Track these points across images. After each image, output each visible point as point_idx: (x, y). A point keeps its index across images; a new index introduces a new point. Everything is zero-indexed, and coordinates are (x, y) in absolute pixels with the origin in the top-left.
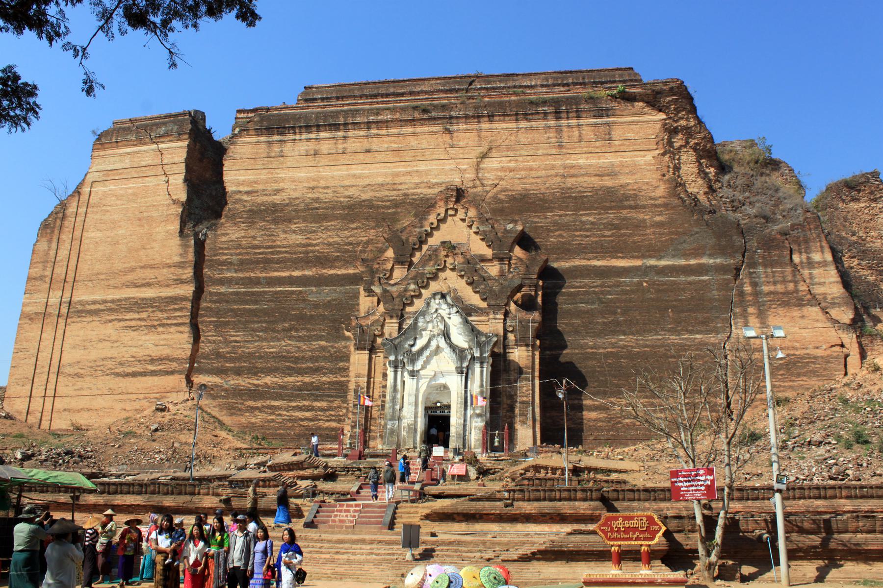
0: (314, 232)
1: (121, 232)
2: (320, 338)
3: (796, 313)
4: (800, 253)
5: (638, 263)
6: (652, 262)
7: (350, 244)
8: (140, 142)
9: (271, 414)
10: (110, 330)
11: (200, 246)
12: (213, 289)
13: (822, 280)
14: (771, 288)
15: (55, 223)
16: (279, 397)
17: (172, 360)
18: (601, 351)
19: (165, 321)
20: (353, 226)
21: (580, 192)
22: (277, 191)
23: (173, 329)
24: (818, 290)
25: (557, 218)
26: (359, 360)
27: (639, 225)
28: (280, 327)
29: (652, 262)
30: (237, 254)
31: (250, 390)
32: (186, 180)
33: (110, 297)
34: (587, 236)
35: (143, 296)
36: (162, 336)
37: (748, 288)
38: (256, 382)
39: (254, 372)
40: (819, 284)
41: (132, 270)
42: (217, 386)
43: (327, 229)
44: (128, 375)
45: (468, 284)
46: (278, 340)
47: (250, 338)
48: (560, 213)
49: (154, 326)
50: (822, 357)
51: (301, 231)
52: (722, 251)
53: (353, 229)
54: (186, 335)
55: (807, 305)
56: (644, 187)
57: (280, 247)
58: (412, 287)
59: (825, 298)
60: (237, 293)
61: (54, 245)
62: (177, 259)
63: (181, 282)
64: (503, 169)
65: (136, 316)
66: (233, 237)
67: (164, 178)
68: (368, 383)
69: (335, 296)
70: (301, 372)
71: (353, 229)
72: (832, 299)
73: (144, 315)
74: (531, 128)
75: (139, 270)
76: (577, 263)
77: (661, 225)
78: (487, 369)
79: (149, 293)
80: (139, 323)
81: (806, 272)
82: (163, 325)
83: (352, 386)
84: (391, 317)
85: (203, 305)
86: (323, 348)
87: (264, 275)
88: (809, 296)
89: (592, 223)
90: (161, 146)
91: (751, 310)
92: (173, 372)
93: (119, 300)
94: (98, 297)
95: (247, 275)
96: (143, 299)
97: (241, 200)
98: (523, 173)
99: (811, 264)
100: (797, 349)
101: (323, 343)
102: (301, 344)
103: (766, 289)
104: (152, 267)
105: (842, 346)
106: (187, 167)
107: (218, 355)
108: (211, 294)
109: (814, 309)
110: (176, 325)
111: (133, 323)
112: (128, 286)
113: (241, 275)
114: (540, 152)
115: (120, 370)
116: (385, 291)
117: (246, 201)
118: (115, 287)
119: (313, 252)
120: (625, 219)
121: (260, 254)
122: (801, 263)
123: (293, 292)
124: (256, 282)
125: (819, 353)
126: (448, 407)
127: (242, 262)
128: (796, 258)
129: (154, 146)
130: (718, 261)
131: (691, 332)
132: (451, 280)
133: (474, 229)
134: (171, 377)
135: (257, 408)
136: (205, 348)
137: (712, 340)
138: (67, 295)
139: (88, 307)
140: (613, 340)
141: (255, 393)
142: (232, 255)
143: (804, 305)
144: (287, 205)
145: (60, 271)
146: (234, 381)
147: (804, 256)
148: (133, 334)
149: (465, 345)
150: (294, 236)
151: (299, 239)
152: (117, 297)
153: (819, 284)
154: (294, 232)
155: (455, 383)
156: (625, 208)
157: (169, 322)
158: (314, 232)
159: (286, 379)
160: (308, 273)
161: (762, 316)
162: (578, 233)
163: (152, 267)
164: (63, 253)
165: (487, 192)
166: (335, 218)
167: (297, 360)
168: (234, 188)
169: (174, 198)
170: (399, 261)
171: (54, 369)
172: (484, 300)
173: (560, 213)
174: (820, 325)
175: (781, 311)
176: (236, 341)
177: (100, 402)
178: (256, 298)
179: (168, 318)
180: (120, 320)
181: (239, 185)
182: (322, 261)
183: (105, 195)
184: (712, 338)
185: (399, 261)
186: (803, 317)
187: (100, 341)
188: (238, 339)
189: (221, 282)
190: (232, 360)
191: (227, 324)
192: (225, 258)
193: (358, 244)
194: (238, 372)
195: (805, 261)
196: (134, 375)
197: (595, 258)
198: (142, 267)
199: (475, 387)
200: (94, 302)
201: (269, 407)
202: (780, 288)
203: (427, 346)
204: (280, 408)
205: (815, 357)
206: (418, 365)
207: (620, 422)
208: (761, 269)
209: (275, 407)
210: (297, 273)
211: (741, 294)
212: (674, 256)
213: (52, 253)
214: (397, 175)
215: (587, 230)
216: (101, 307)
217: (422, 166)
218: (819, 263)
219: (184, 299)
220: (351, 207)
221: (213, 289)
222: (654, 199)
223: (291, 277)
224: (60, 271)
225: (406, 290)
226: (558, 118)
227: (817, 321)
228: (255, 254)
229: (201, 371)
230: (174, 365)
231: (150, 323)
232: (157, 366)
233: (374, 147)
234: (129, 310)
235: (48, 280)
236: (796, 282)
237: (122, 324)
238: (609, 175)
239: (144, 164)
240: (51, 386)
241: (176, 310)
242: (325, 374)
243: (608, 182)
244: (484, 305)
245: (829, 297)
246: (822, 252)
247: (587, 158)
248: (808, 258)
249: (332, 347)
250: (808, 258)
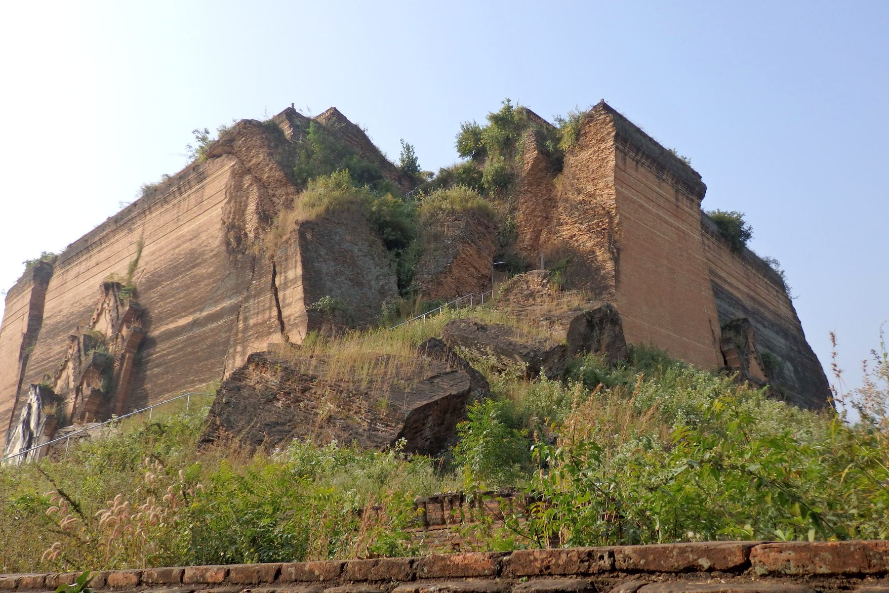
5: (190, 319)
6: (198, 315)
29: (198, 315)
34: (172, 302)
52: (237, 290)
55: (273, 332)
59: (289, 320)
72: (295, 319)
76: (163, 329)
77: (210, 275)
103: (251, 322)
120: (195, 276)
147: (283, 278)
212: (210, 305)
226: (181, 194)
238: (195, 237)
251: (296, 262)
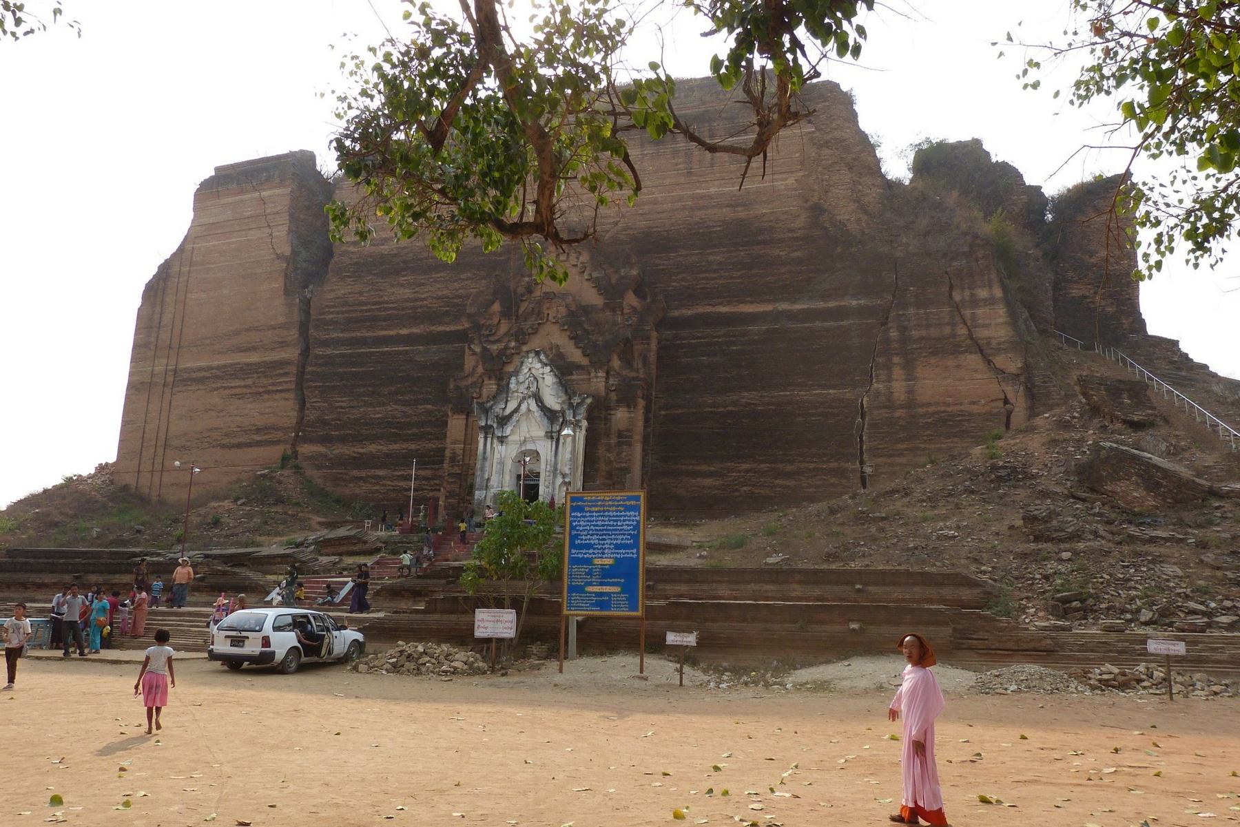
0: (423, 284)
1: (225, 292)
2: (427, 401)
3: (951, 362)
4: (963, 289)
5: (768, 308)
6: (784, 306)
7: (460, 297)
8: (242, 192)
9: (374, 484)
11: (307, 303)
12: (319, 351)
13: (987, 322)
14: (923, 333)
16: (383, 466)
17: (277, 429)
18: (721, 409)
19: (271, 388)
20: (463, 276)
21: (708, 227)
23: (278, 396)
24: (981, 334)
25: (681, 259)
26: (456, 424)
29: (784, 306)
30: (343, 312)
31: (354, 458)
32: (290, 231)
33: (215, 363)
35: (248, 360)
36: (268, 404)
37: (894, 334)
38: (361, 451)
39: (360, 439)
40: (983, 326)
41: (237, 333)
42: (321, 455)
43: (435, 281)
45: (571, 338)
46: (384, 404)
47: (356, 404)
48: (684, 252)
49: (260, 394)
50: (979, 414)
53: (463, 280)
54: (291, 403)
56: (783, 217)
57: (387, 302)
58: (513, 344)
59: (989, 343)
60: (343, 355)
61: (158, 309)
62: (282, 319)
63: (284, 344)
65: (242, 383)
66: (341, 292)
67: (268, 231)
68: (464, 449)
70: (406, 439)
71: (463, 280)
72: (999, 344)
73: (249, 382)
78: (581, 435)
79: (254, 358)
80: (245, 390)
81: (967, 313)
82: (269, 392)
83: (448, 453)
84: (490, 378)
85: (309, 369)
86: (429, 412)
87: (370, 334)
88: (968, 342)
89: (720, 263)
90: (263, 194)
91: (896, 359)
92: (278, 442)
93: (225, 366)
94: (202, 364)
95: (353, 335)
96: (248, 364)
97: (346, 252)
99: (975, 302)
100: (949, 405)
101: (429, 407)
102: (406, 409)
103: (915, 333)
104: (256, 329)
105: (1006, 401)
106: (292, 216)
107: (325, 423)
108: (317, 357)
109: (973, 356)
110: (281, 391)
111: (238, 391)
112: (233, 351)
113: (347, 335)
114: (667, 181)
115: (226, 441)
116: (484, 349)
117: (353, 253)
118: (220, 353)
119: (421, 307)
121: (366, 311)
122: (963, 300)
123: (399, 353)
124: (363, 342)
125: (975, 409)
126: (538, 475)
128: (957, 296)
130: (862, 302)
131: (823, 387)
132: (557, 337)
134: (277, 447)
135: (361, 478)
136: (311, 415)
137: (848, 396)
138: (173, 362)
139: (194, 375)
140: (735, 398)
141: (359, 462)
142: (338, 313)
143: (962, 353)
144: (395, 255)
145: (165, 336)
146: (340, 450)
147: (967, 293)
149: (557, 407)
150: (402, 291)
151: (407, 293)
152: (222, 362)
153: (983, 326)
154: (402, 285)
155: (545, 448)
156: (759, 243)
157: (275, 388)
158: (423, 284)
159: (391, 447)
160: (415, 330)
161: (909, 367)
162: (702, 276)
163: (256, 329)
165: (607, 231)
169: (279, 252)
170: (506, 314)
171: (161, 442)
172: (585, 355)
173: (684, 252)
174: (980, 376)
175: (933, 360)
176: (341, 407)
179: (274, 384)
180: (225, 388)
182: (432, 317)
184: (847, 394)
185: (506, 314)
186: (958, 367)
187: (207, 410)
188: (343, 404)
189: (326, 343)
193: (468, 297)
194: (343, 440)
195: (967, 298)
196: (239, 446)
197: (721, 304)
198: (247, 330)
199: (566, 453)
200: (200, 369)
201: (375, 477)
202: (933, 332)
203: (516, 410)
204: (384, 478)
205: (970, 414)
206: (508, 430)
207: (737, 490)
208: (911, 311)
209: (379, 477)
210: (404, 332)
213: (156, 317)
215: (714, 271)
216: (207, 374)
218: (985, 300)
219: (289, 363)
221: (319, 351)
222: (791, 230)
223: (398, 335)
224: (165, 336)
225: (506, 348)
227: (976, 371)
228: (362, 311)
229: (306, 440)
230: (280, 434)
231: (254, 390)
232: (261, 435)
234: (234, 376)
235: (153, 347)
236: (953, 325)
237: (228, 392)
240: (159, 460)
241: (282, 375)
242: (430, 440)
243: (741, 214)
244: (585, 361)
245: (994, 342)
246: (990, 287)
247: (720, 186)
248: (972, 295)
249: (439, 411)
250: (972, 295)
251: (990, 281)
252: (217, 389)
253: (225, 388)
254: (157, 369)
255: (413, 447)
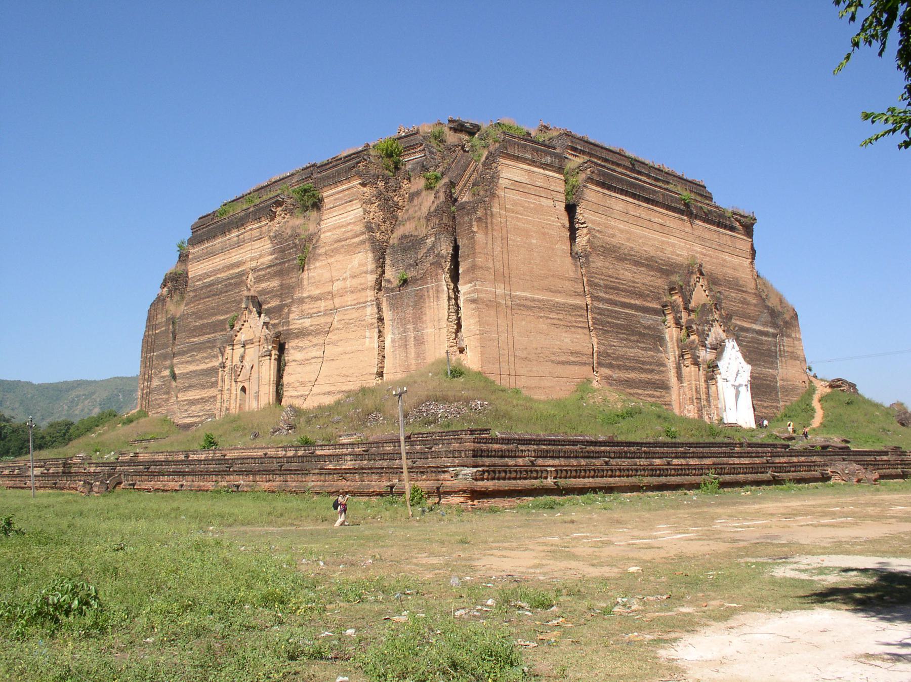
10: (542, 325)
15: (486, 219)
22: (613, 236)
23: (580, 330)
27: (748, 304)
28: (632, 338)
33: (536, 296)
36: (575, 336)
39: (627, 369)
44: (559, 363)
51: (630, 271)
60: (608, 310)
61: (490, 242)
62: (572, 274)
64: (701, 253)
66: (599, 264)
69: (652, 322)
73: (561, 317)
74: (709, 229)
75: (551, 279)
77: (755, 305)
79: (560, 299)
80: (559, 322)
86: (653, 357)
90: (547, 172)
92: (585, 364)
94: (528, 295)
96: (558, 303)
98: (708, 259)
111: (556, 322)
113: (607, 296)
115: (553, 358)
118: (538, 289)
123: (633, 315)
127: (606, 286)
129: (541, 171)
133: (707, 293)
139: (524, 303)
144: (619, 248)
146: (617, 374)
148: (556, 330)
151: (628, 275)
156: (743, 291)
164: (498, 250)
166: (643, 265)
167: (643, 363)
168: (590, 225)
177: (547, 383)
178: (617, 315)
179: (576, 322)
180: (547, 318)
181: (593, 222)
183: (515, 204)
190: (614, 359)
191: (608, 331)
192: (596, 280)
194: (619, 367)
196: (563, 363)
200: (526, 299)
201: (637, 394)
210: (633, 302)
211: (780, 351)
214: (663, 242)
217: (672, 240)
219: (582, 308)
220: (647, 259)
230: (585, 358)
231: (565, 324)
232: (574, 358)
233: (653, 219)
235: (492, 271)
237: (549, 321)
239: (539, 184)
243: (737, 274)
252: (541, 317)
253: (547, 318)
254: (498, 291)
255: (650, 377)
